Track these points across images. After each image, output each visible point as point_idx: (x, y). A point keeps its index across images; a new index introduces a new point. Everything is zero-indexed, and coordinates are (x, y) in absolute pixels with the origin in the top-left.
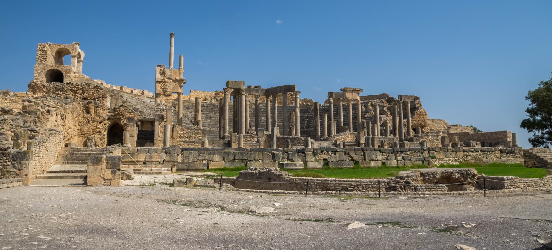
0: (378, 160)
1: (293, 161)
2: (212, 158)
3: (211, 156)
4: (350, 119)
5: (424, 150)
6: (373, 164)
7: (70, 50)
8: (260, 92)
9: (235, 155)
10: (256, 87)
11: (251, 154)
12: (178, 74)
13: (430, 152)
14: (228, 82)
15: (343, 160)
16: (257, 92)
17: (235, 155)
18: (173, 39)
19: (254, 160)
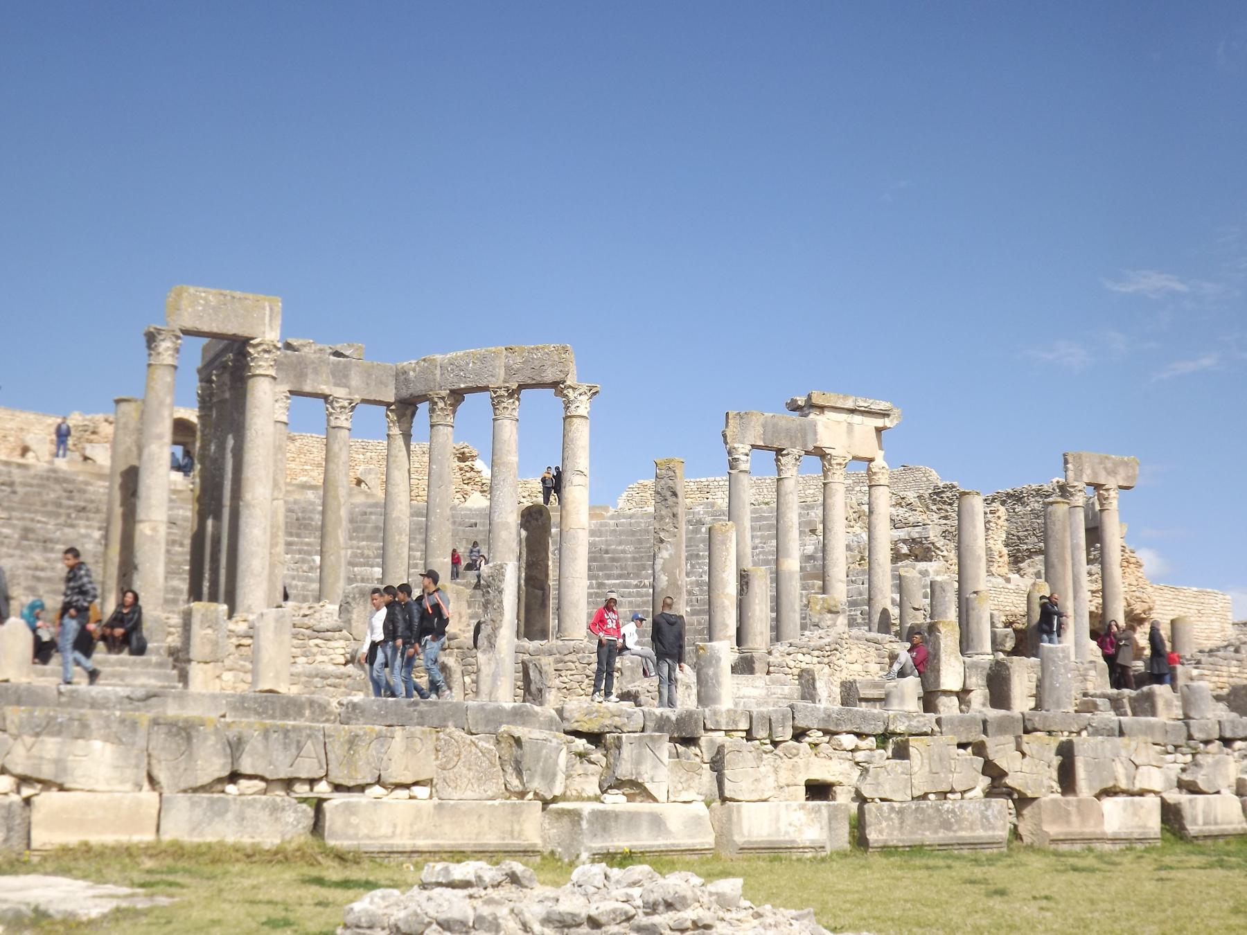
0: (1142, 793)
2: (59, 763)
3: (50, 746)
6: (1115, 817)
8: (356, 380)
9: (235, 747)
11: (352, 741)
17: (235, 747)
19: (379, 781)
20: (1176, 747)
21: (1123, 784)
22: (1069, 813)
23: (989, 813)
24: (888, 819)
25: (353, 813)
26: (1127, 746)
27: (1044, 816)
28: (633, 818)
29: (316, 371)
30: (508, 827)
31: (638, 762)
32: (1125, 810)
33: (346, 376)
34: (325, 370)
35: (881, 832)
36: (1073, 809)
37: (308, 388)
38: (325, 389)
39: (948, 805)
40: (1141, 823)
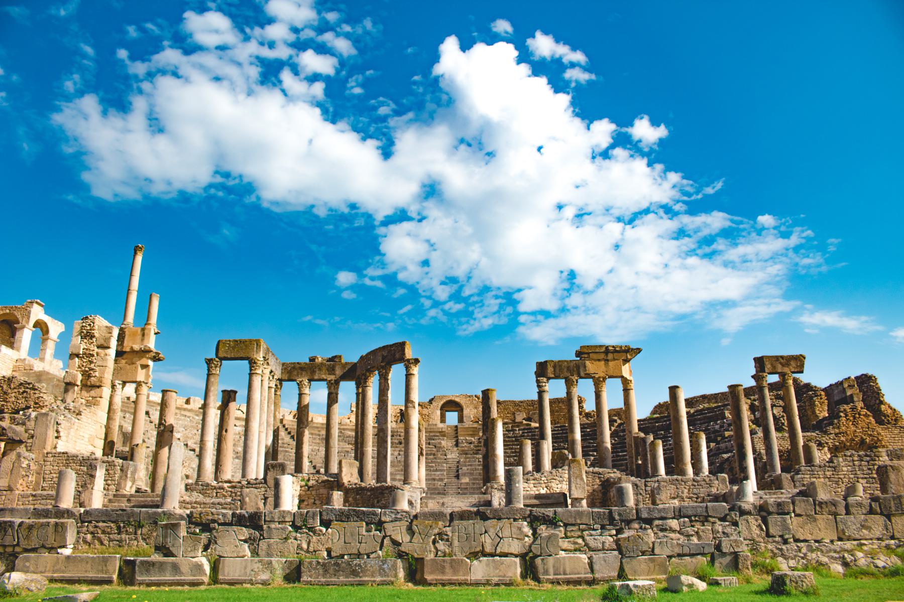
0: (506, 555)
1: (173, 556)
4: (602, 433)
5: (743, 513)
7: (19, 317)
10: (330, 360)
12: (139, 337)
13: (771, 519)
14: (219, 342)
15: (359, 555)
16: (331, 370)
18: (139, 258)
19: (43, 546)
20: (603, 527)
21: (488, 549)
22: (444, 567)
23: (386, 566)
24: (315, 569)
25: (28, 561)
26: (494, 526)
27: (426, 570)
28: (161, 566)
29: (320, 369)
30: (100, 568)
31: (165, 537)
32: (487, 565)
33: (334, 370)
34: (324, 368)
35: (310, 576)
36: (447, 566)
37: (316, 377)
38: (324, 377)
39: (357, 561)
40: (501, 574)
